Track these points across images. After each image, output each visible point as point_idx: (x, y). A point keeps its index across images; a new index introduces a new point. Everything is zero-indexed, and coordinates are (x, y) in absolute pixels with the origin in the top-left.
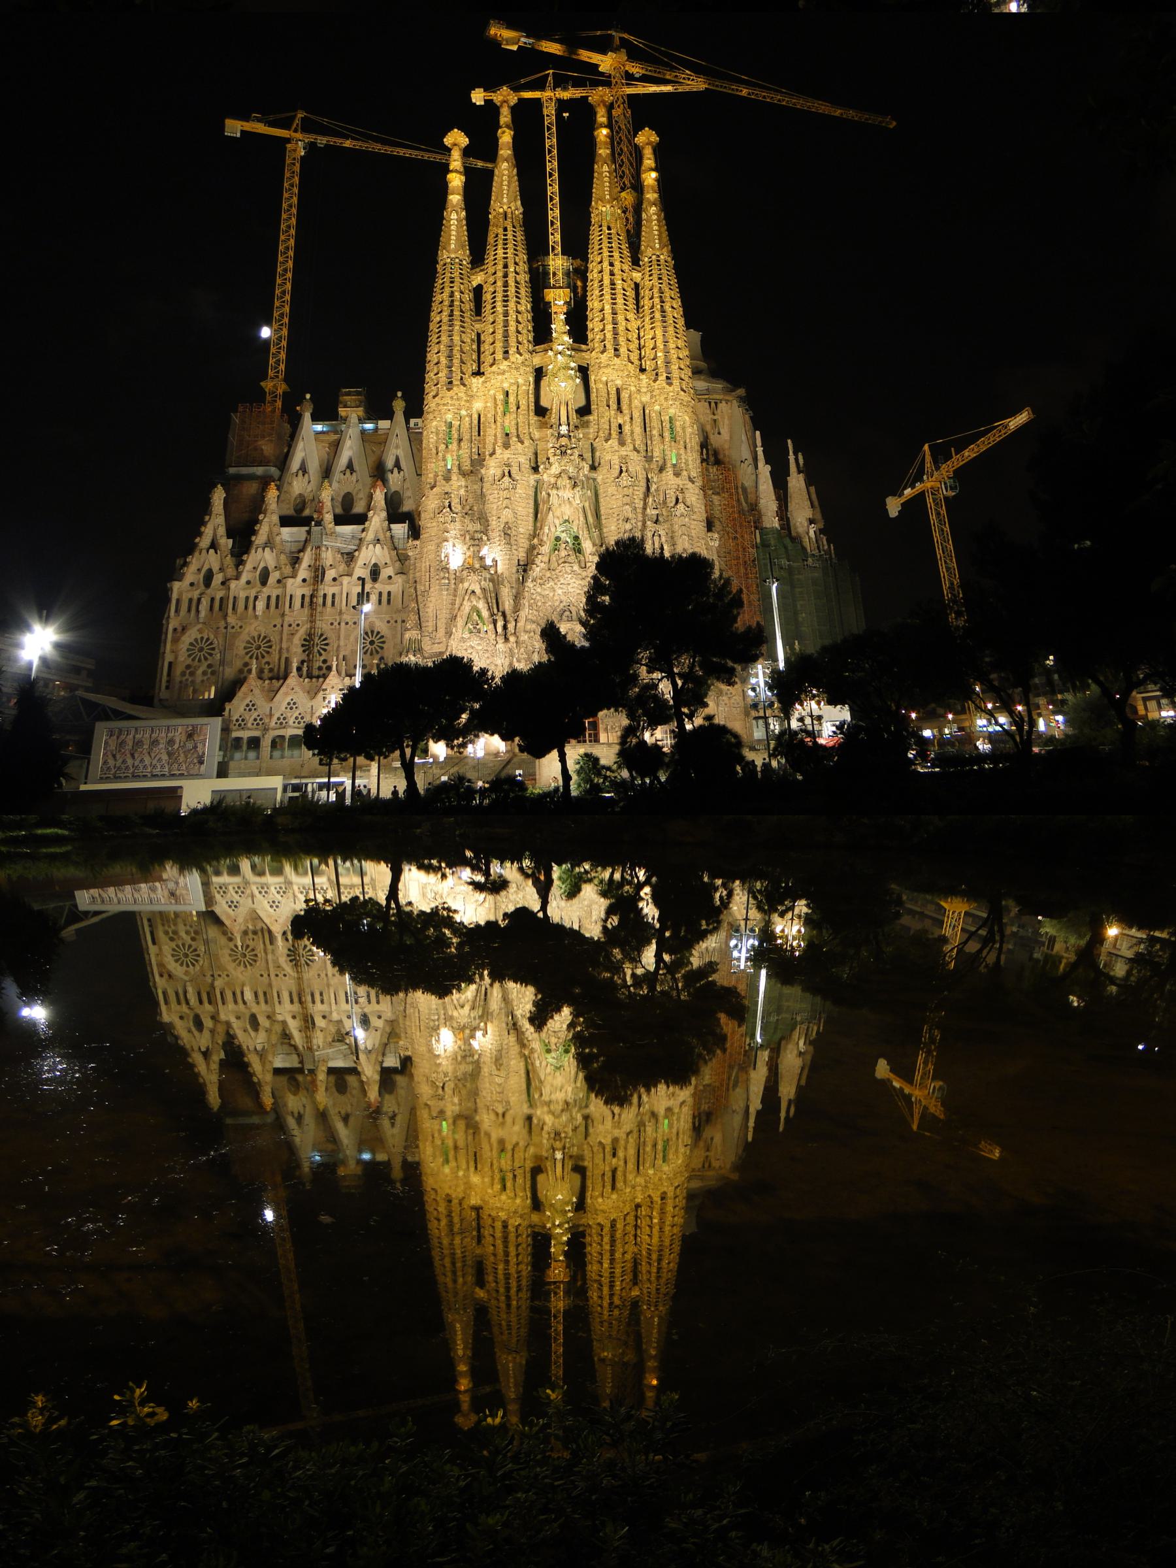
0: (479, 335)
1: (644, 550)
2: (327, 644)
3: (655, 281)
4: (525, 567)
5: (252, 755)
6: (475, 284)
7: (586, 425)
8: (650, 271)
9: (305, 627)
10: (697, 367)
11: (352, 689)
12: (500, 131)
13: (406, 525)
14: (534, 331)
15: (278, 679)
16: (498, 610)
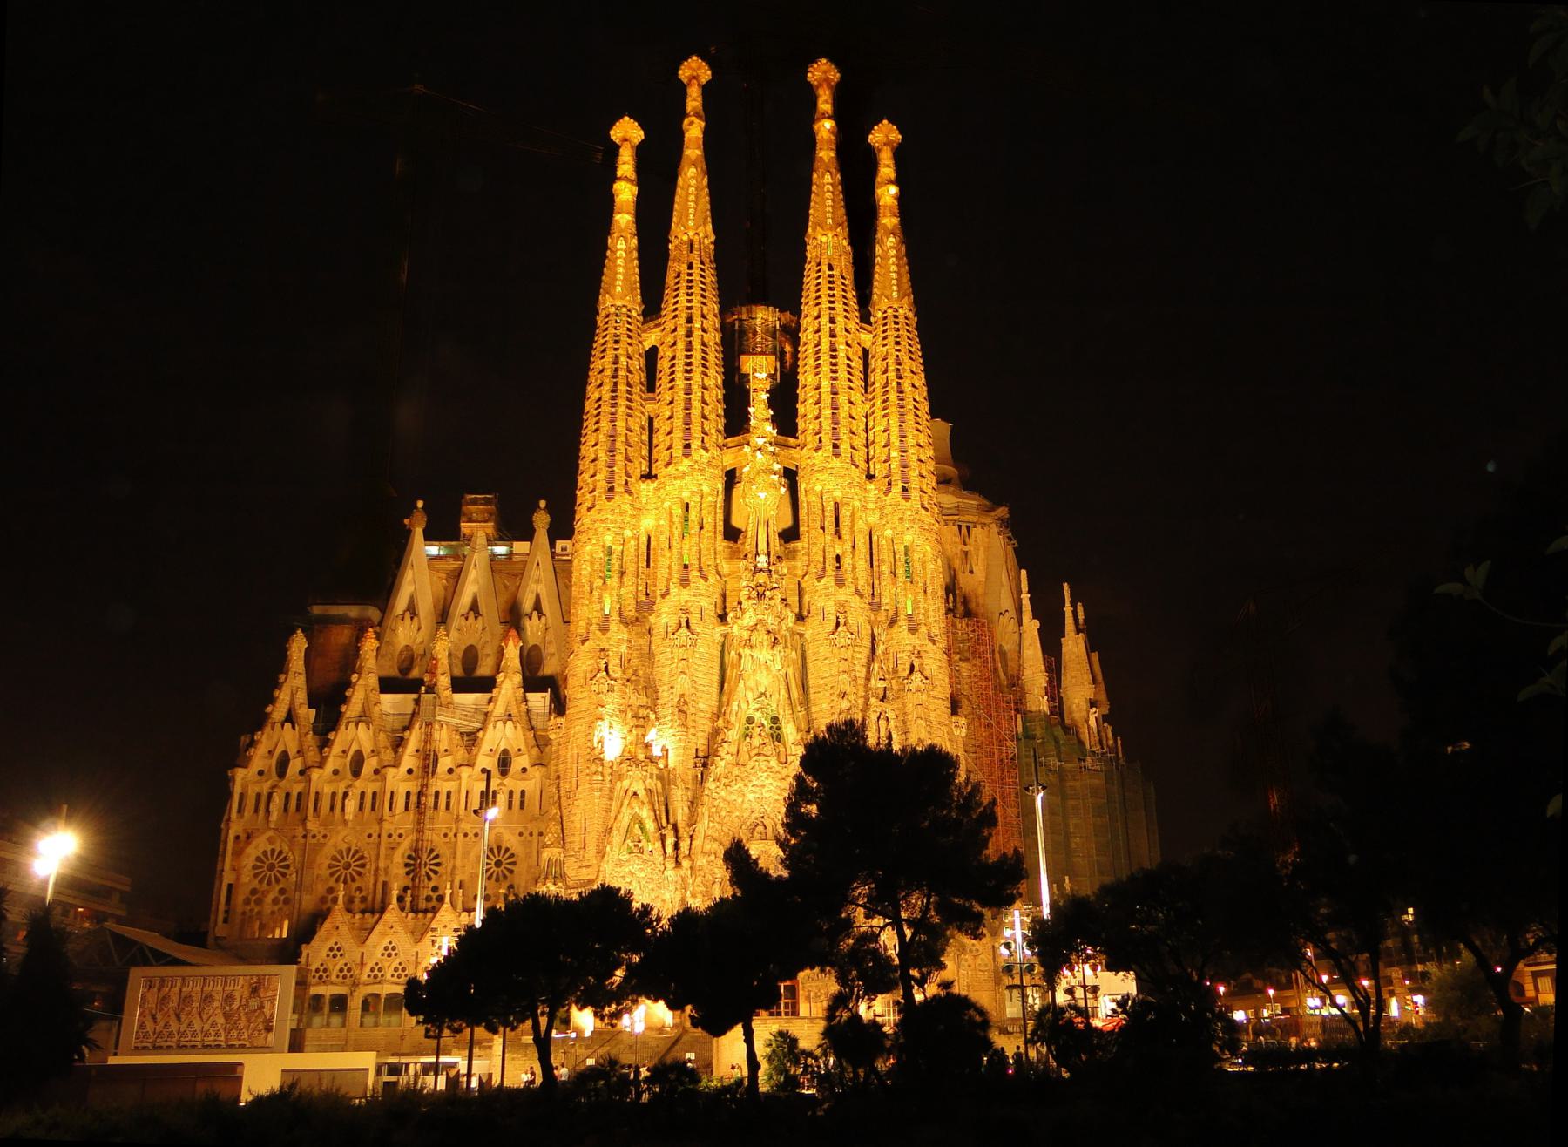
0: (651, 420)
1: (865, 739)
2: (438, 865)
3: (891, 347)
4: (705, 760)
5: (336, 1020)
6: (647, 346)
7: (792, 555)
8: (884, 332)
9: (410, 838)
10: (944, 475)
11: (470, 929)
12: (686, 121)
13: (547, 695)
14: (725, 417)
15: (373, 912)
16: (668, 822)
